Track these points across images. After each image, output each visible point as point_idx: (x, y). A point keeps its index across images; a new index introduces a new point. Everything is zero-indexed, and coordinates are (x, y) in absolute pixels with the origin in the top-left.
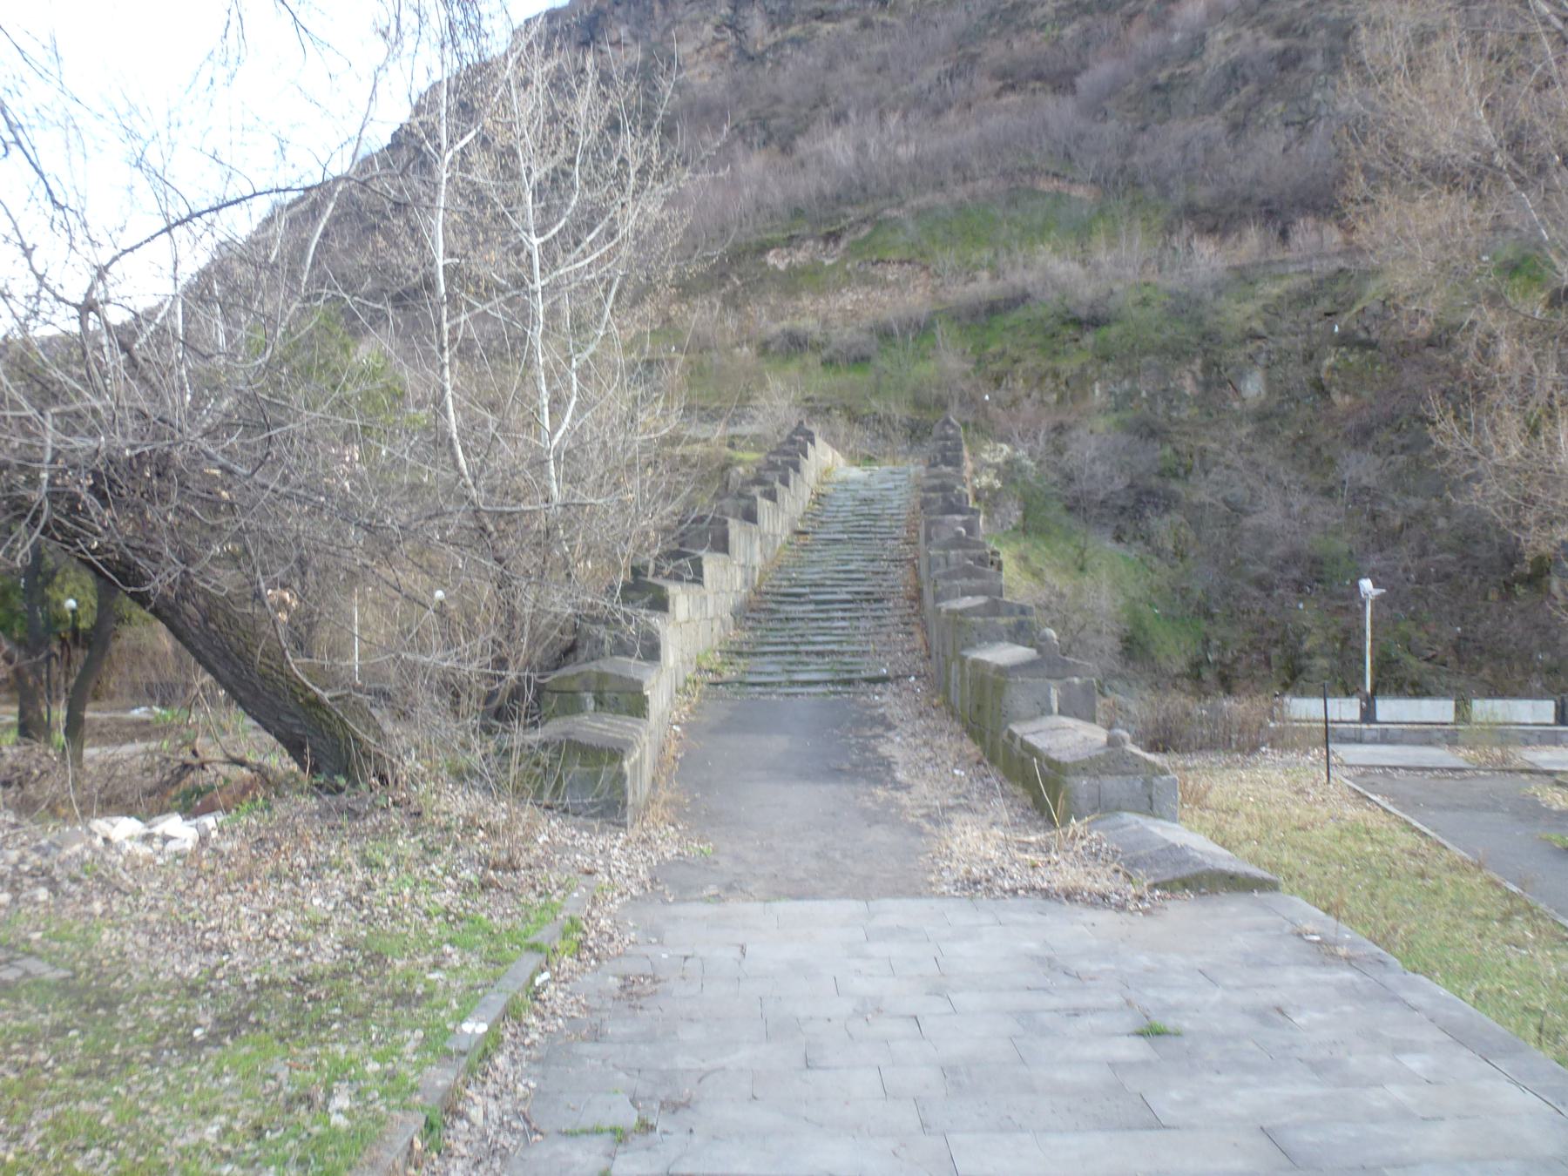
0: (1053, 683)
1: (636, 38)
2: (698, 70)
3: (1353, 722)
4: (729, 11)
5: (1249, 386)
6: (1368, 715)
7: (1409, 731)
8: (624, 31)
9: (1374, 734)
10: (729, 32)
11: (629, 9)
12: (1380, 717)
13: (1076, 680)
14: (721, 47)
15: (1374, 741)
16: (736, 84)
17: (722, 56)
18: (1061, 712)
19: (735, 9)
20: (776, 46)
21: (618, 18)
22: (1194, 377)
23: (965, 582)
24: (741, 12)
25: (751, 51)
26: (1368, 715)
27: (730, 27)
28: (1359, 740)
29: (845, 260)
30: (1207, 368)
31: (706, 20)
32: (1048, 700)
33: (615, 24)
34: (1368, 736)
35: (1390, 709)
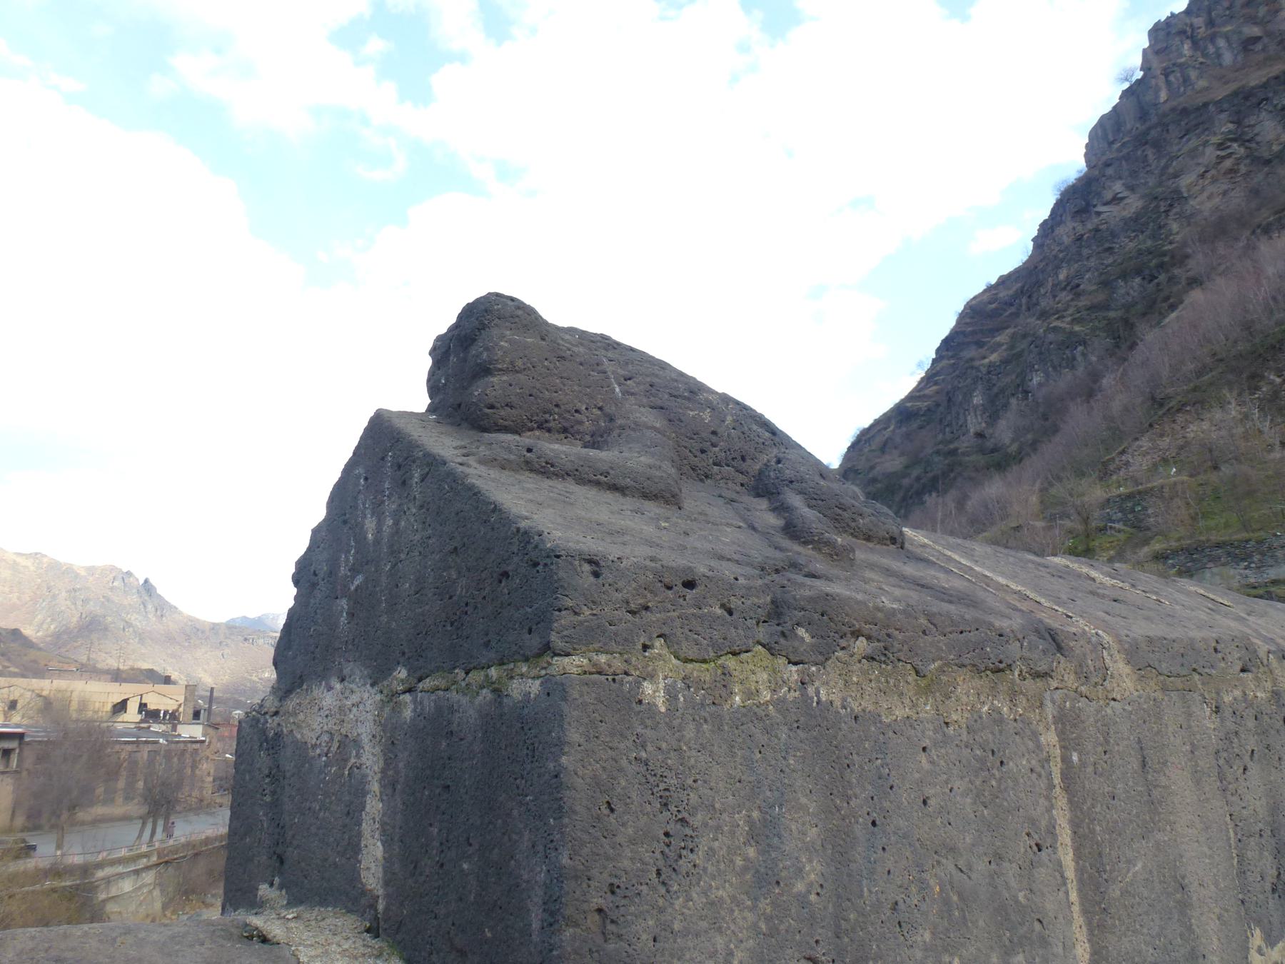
1: (1132, 189)
2: (1205, 194)
4: (1231, 126)
8: (1118, 187)
10: (1235, 145)
14: (1228, 163)
16: (1255, 192)
17: (1232, 171)
19: (1238, 123)
21: (1110, 177)
24: (1246, 122)
25: (1266, 155)
27: (1234, 140)
31: (1205, 144)
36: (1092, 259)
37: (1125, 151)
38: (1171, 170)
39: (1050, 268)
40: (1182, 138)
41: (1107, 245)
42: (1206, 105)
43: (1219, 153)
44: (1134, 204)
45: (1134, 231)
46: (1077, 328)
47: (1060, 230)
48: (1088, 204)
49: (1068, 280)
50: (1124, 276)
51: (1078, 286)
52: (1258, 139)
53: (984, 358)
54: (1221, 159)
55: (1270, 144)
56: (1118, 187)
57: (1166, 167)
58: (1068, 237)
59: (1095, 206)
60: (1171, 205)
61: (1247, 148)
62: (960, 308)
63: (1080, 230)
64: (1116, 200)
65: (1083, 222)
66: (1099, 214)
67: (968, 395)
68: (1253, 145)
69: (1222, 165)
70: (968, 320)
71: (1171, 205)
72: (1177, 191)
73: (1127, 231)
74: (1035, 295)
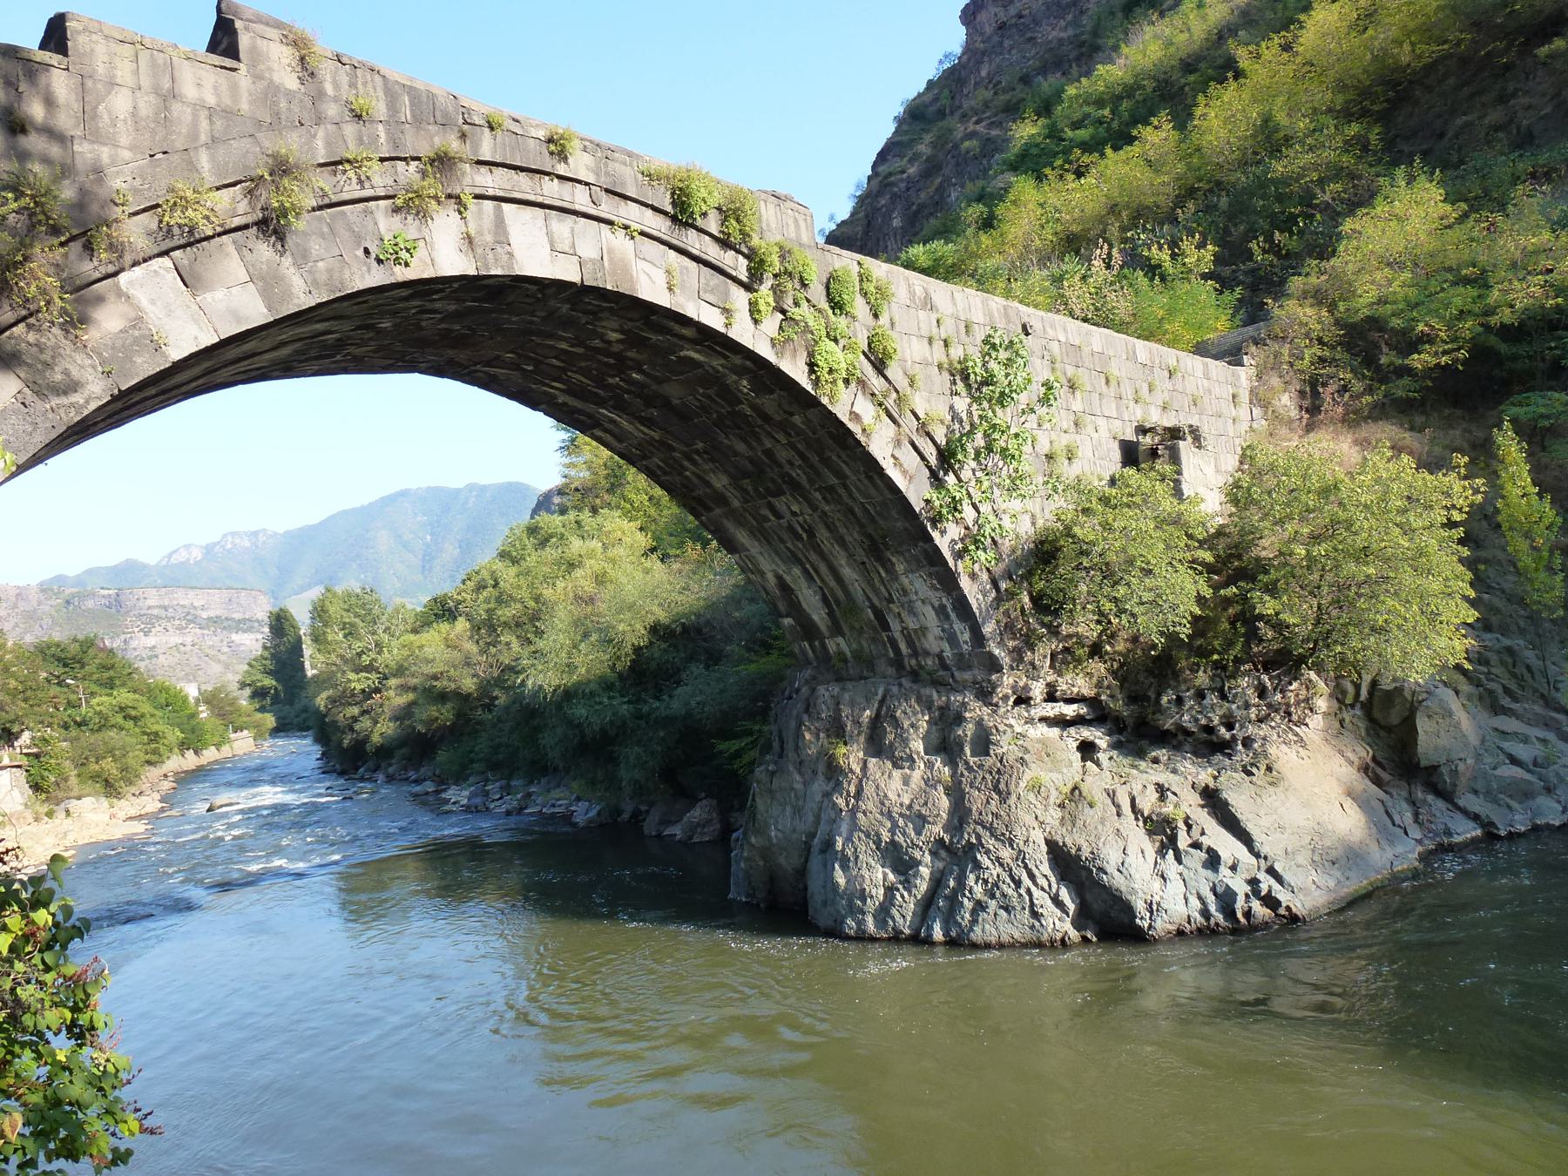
36: (1014, 52)
39: (971, 64)
41: (1029, 35)
46: (994, 133)
47: (983, 17)
49: (990, 77)
53: (903, 172)
62: (899, 110)
63: (1003, 17)
65: (1005, 6)
67: (888, 217)
70: (905, 127)
73: (1049, 18)
74: (958, 96)
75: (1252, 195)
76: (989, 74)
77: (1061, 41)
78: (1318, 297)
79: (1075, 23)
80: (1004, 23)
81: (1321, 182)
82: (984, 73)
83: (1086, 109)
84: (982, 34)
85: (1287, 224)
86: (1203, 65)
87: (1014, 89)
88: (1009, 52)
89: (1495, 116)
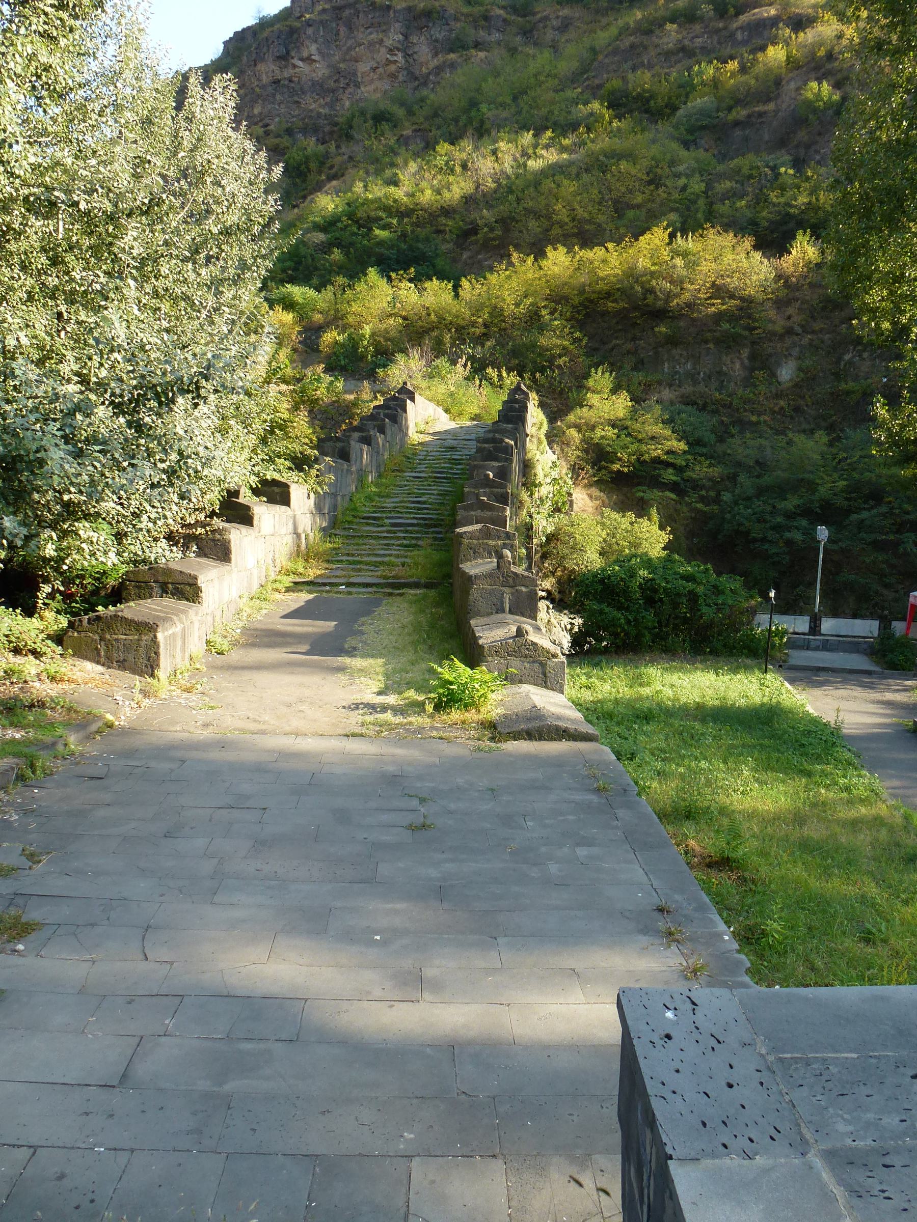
0: (507, 590)
2: (373, 87)
3: (804, 634)
5: (784, 373)
6: (814, 629)
7: (844, 642)
8: (313, 48)
9: (818, 643)
11: (318, 30)
12: (823, 631)
13: (524, 589)
14: (393, 68)
15: (817, 649)
17: (393, 76)
18: (511, 612)
19: (406, 36)
20: (439, 70)
21: (309, 37)
22: (742, 364)
23: (479, 513)
25: (417, 73)
26: (814, 629)
28: (807, 647)
29: (478, 253)
30: (753, 357)
32: (502, 603)
33: (307, 42)
34: (813, 644)
35: (828, 625)
36: (283, 106)
37: (325, 17)
38: (353, 53)
40: (367, 28)
41: (296, 98)
42: (389, 8)
43: (388, 56)
44: (321, 70)
45: (317, 95)
48: (288, 53)
50: (305, 131)
51: (267, 125)
52: (415, 56)
54: (389, 62)
55: (421, 65)
56: (313, 48)
57: (350, 49)
58: (268, 77)
59: (293, 58)
60: (348, 85)
61: (407, 61)
64: (309, 60)
66: (295, 66)
68: (411, 61)
69: (388, 67)
71: (348, 85)
72: (355, 74)
73: (312, 93)
75: (527, 350)
76: (261, 114)
77: (319, 115)
78: (578, 427)
79: (331, 106)
80: (279, 81)
81: (560, 356)
82: (256, 111)
83: (381, 214)
84: (259, 80)
85: (542, 370)
86: (457, 216)
87: (278, 136)
88: (279, 104)
89: (629, 346)
